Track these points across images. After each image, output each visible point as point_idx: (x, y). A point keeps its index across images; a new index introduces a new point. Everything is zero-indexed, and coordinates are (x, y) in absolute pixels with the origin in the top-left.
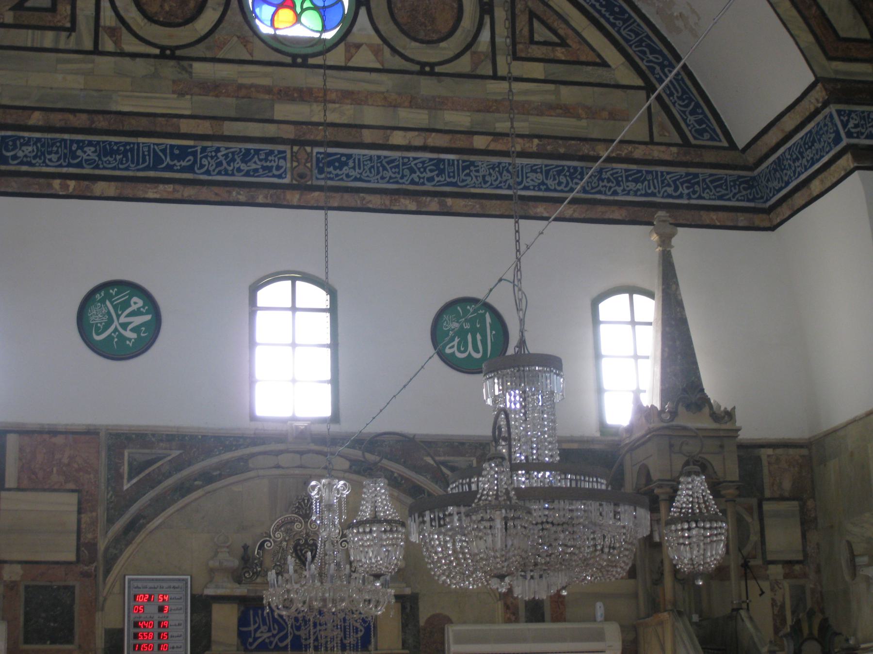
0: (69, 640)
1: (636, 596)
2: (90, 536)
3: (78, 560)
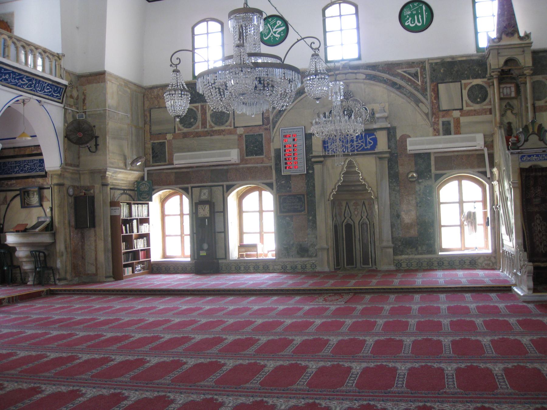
0: (261, 154)
1: (492, 121)
2: (267, 115)
3: (263, 124)
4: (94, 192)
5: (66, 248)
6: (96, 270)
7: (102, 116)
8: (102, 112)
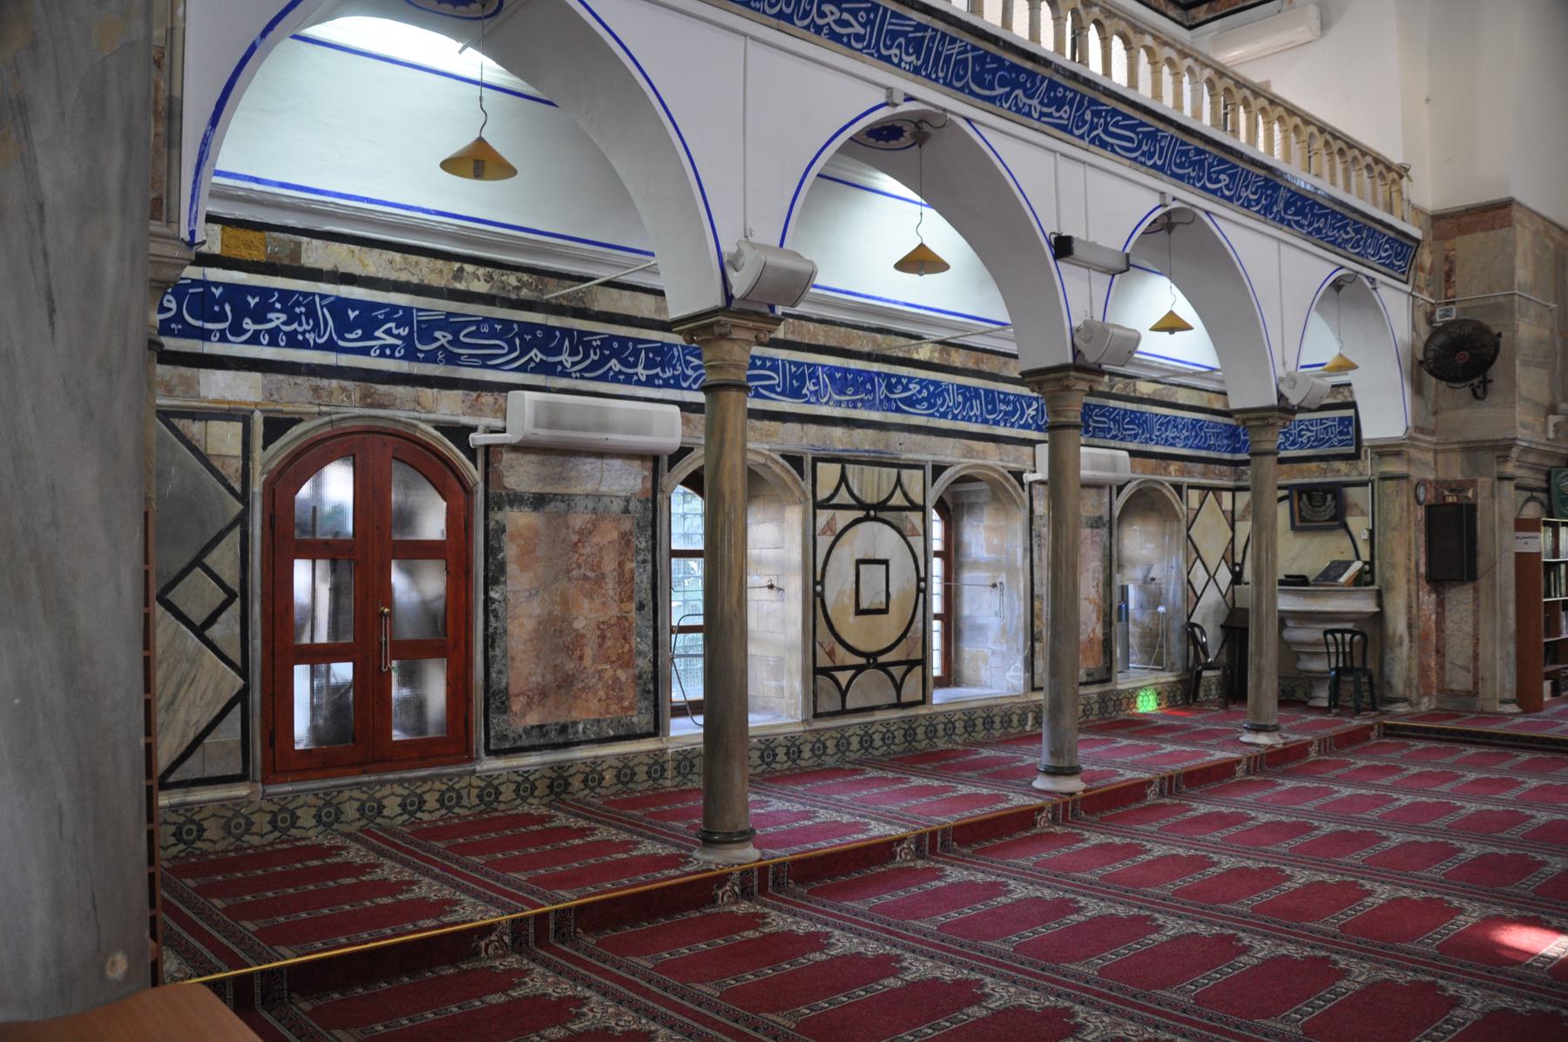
4: (1475, 495)
5: (1410, 626)
6: (1476, 683)
7: (1505, 309)
8: (1502, 300)
